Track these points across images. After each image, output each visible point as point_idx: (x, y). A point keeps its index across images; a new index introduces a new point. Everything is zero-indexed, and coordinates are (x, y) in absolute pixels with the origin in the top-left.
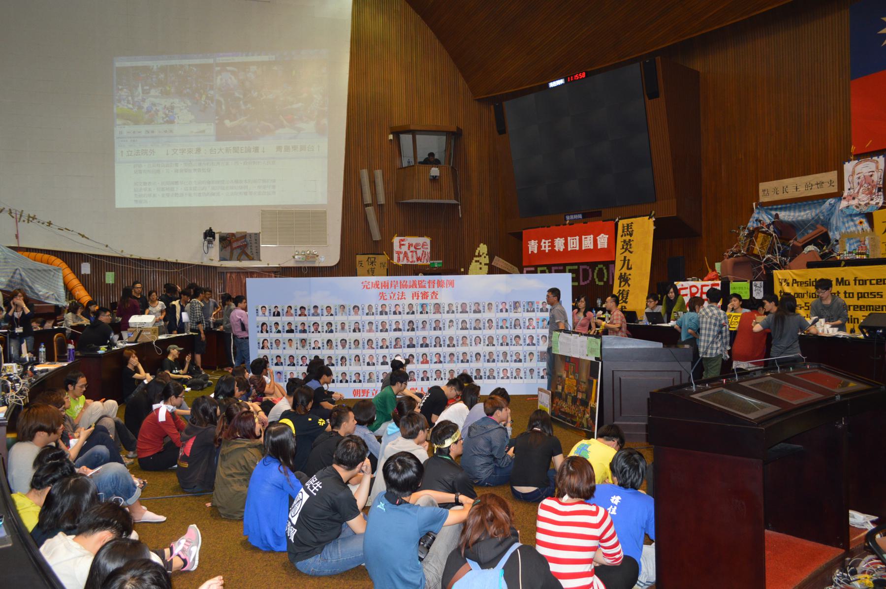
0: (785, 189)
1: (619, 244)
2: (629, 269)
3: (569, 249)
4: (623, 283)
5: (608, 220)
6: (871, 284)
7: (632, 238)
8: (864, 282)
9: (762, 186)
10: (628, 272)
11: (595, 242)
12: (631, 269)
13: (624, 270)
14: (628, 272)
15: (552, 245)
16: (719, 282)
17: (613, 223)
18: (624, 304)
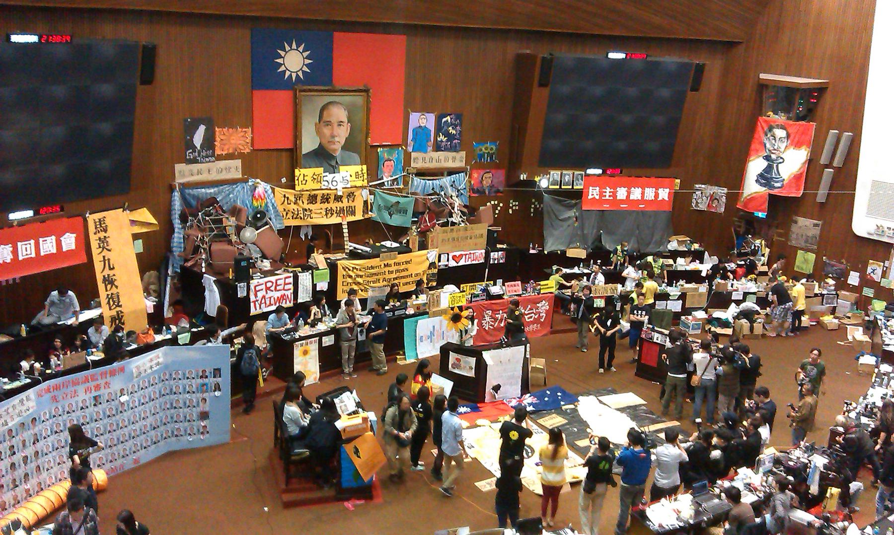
1: (94, 244)
2: (111, 269)
3: (21, 258)
4: (109, 287)
7: (106, 235)
8: (399, 264)
9: (179, 167)
10: (111, 273)
11: (59, 244)
12: (114, 268)
13: (107, 272)
14: (111, 273)
16: (292, 275)
18: (118, 309)
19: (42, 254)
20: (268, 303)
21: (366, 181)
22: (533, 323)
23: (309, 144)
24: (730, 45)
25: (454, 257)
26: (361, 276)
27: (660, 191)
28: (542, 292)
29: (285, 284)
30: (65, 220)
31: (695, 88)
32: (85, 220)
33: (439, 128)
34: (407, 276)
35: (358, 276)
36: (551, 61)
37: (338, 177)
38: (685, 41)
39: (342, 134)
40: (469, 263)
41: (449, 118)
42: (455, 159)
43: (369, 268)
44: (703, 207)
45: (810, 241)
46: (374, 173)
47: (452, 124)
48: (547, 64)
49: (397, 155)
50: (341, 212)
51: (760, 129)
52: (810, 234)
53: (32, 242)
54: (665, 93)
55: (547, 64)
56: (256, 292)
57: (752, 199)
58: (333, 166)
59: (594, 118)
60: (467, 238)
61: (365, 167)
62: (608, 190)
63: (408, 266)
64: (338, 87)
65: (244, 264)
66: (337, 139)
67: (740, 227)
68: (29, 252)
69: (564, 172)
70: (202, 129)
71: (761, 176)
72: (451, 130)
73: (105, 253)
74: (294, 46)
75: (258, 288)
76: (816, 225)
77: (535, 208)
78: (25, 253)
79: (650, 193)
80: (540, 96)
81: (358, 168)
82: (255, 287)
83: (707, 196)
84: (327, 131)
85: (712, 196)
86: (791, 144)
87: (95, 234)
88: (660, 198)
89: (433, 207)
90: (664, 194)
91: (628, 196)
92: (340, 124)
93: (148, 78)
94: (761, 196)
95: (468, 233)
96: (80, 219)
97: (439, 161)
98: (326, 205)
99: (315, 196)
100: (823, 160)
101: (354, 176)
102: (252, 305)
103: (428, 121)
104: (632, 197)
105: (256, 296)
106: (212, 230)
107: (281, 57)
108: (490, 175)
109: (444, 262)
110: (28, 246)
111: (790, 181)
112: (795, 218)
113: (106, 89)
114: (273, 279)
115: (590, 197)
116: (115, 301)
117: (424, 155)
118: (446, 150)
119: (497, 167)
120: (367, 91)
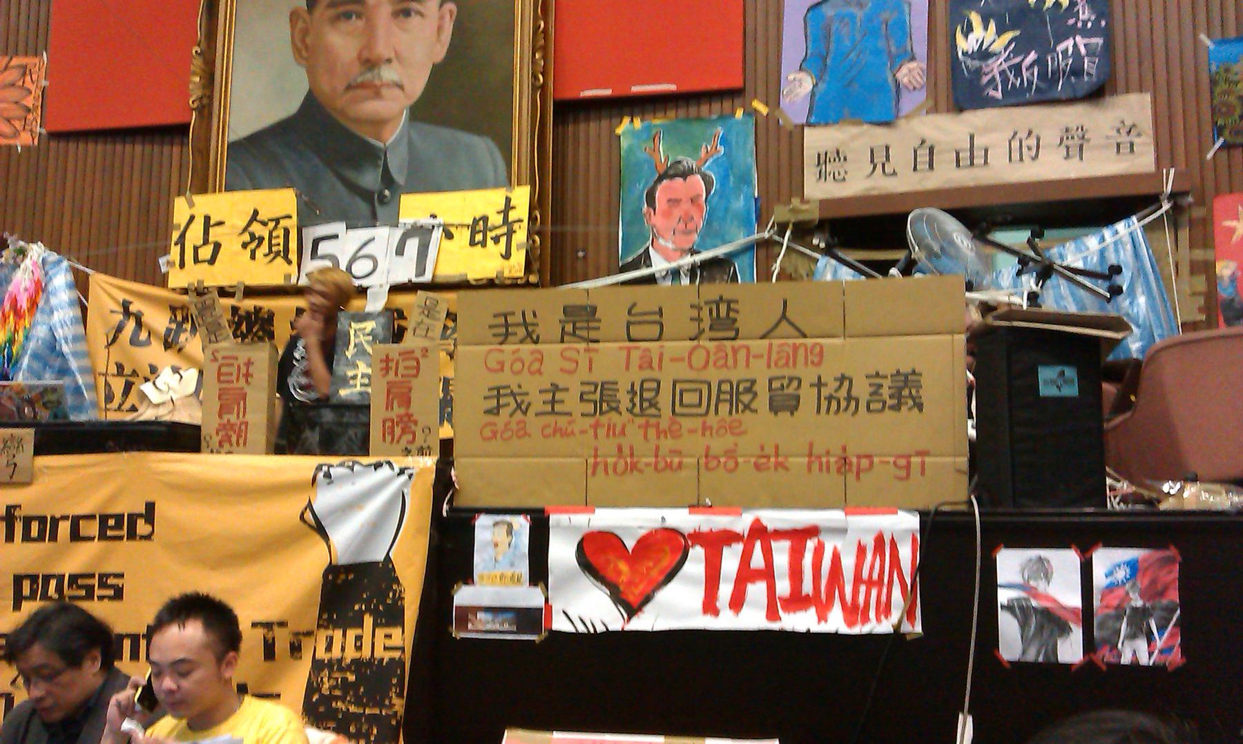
6: (76, 536)
8: (46, 528)
21: (519, 258)
23: (258, 93)
25: (597, 554)
37: (384, 236)
40: (753, 618)
58: (367, 195)
60: (738, 396)
61: (521, 196)
63: (120, 557)
66: (388, 74)
81: (487, 202)
84: (342, 43)
95: (755, 360)
101: (463, 236)
109: (494, 582)
117: (880, 136)
118: (1016, 97)
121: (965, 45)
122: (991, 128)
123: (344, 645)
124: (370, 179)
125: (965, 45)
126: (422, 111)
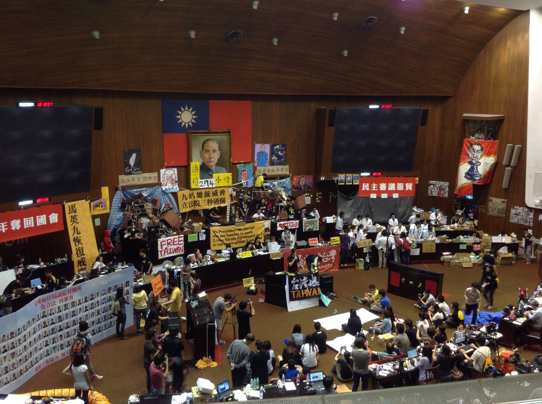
0: (133, 179)
2: (78, 234)
3: (25, 227)
4: (77, 244)
5: (57, 204)
7: (76, 214)
8: (247, 229)
9: (121, 177)
10: (79, 236)
11: (48, 220)
12: (80, 233)
14: (79, 236)
15: (9, 226)
17: (60, 205)
18: (82, 256)
19: (38, 225)
20: (169, 251)
22: (327, 263)
24: (444, 99)
25: (280, 225)
26: (224, 236)
27: (407, 185)
28: (332, 244)
29: (179, 241)
30: (52, 205)
31: (424, 123)
32: (64, 207)
33: (272, 152)
34: (252, 236)
35: (222, 236)
36: (335, 110)
37: (213, 180)
38: (418, 97)
39: (216, 157)
41: (278, 146)
42: (284, 170)
43: (228, 231)
44: (435, 194)
45: (500, 212)
46: (235, 179)
47: (280, 150)
48: (333, 113)
49: (250, 167)
50: (217, 201)
51: (465, 146)
52: (500, 207)
53: (32, 218)
54: (405, 127)
55: (333, 113)
56: (162, 246)
57: (463, 188)
59: (363, 143)
62: (374, 185)
63: (253, 230)
64: (213, 131)
65: (153, 230)
66: (213, 160)
67: (458, 205)
68: (30, 224)
69: (347, 175)
70: (134, 156)
71: (467, 173)
72: (280, 153)
73: (75, 224)
74: (187, 108)
75: (163, 243)
76: (503, 202)
77: (332, 197)
78: (28, 224)
79: (400, 187)
80: (329, 132)
82: (161, 243)
83: (437, 188)
84: (206, 155)
85: (440, 187)
86: (485, 154)
87: (69, 213)
88: (407, 189)
89: (269, 197)
90: (409, 187)
91: (387, 188)
92: (214, 151)
93: (99, 126)
94: (468, 186)
96: (60, 205)
97: (273, 171)
98: (208, 198)
99: (201, 193)
100: (504, 162)
102: (159, 253)
103: (267, 148)
104: (389, 189)
105: (162, 248)
106: (138, 211)
107: (179, 115)
108: (304, 178)
110: (30, 220)
111: (485, 176)
112: (490, 198)
113: (75, 132)
114: (172, 238)
115: (363, 189)
116: (80, 252)
117: (264, 168)
118: (277, 164)
119: (308, 173)
120: (229, 132)
121: (273, 158)
122: (275, 167)
123: (266, 233)
124: (211, 173)
125: (273, 158)
126: (217, 165)
